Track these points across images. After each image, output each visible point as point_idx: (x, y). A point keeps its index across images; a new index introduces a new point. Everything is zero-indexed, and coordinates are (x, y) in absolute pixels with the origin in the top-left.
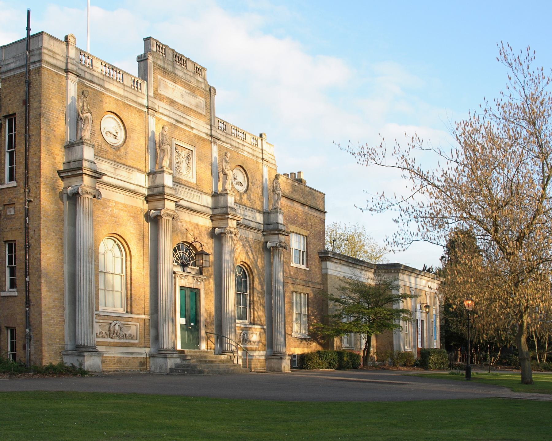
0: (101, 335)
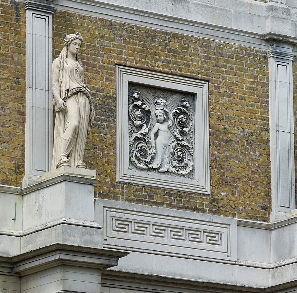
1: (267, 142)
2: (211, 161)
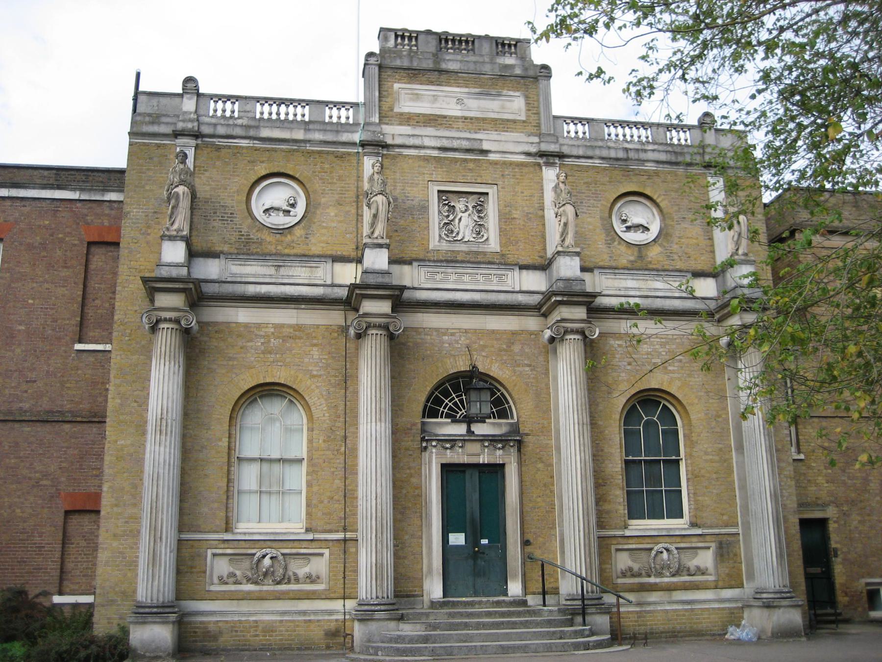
0: (232, 580)
1: (543, 217)
2: (500, 232)
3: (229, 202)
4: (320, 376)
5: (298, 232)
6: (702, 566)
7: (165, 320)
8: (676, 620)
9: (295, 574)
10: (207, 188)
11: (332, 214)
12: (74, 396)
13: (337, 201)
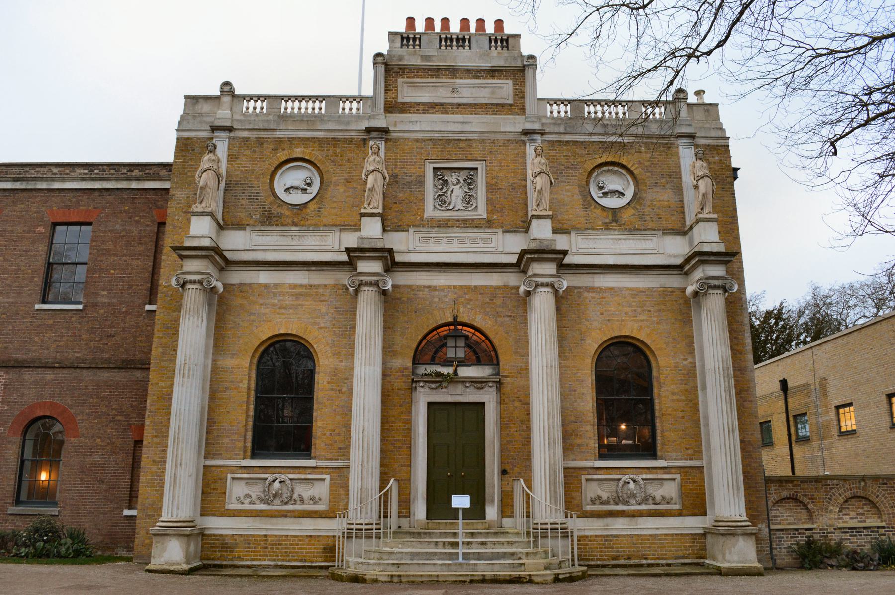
0: (248, 500)
3: (255, 184)
4: (326, 328)
5: (312, 206)
6: (667, 496)
7: (191, 282)
8: (641, 544)
9: (300, 496)
10: (238, 173)
11: (341, 190)
12: (144, 347)
13: (346, 179)
